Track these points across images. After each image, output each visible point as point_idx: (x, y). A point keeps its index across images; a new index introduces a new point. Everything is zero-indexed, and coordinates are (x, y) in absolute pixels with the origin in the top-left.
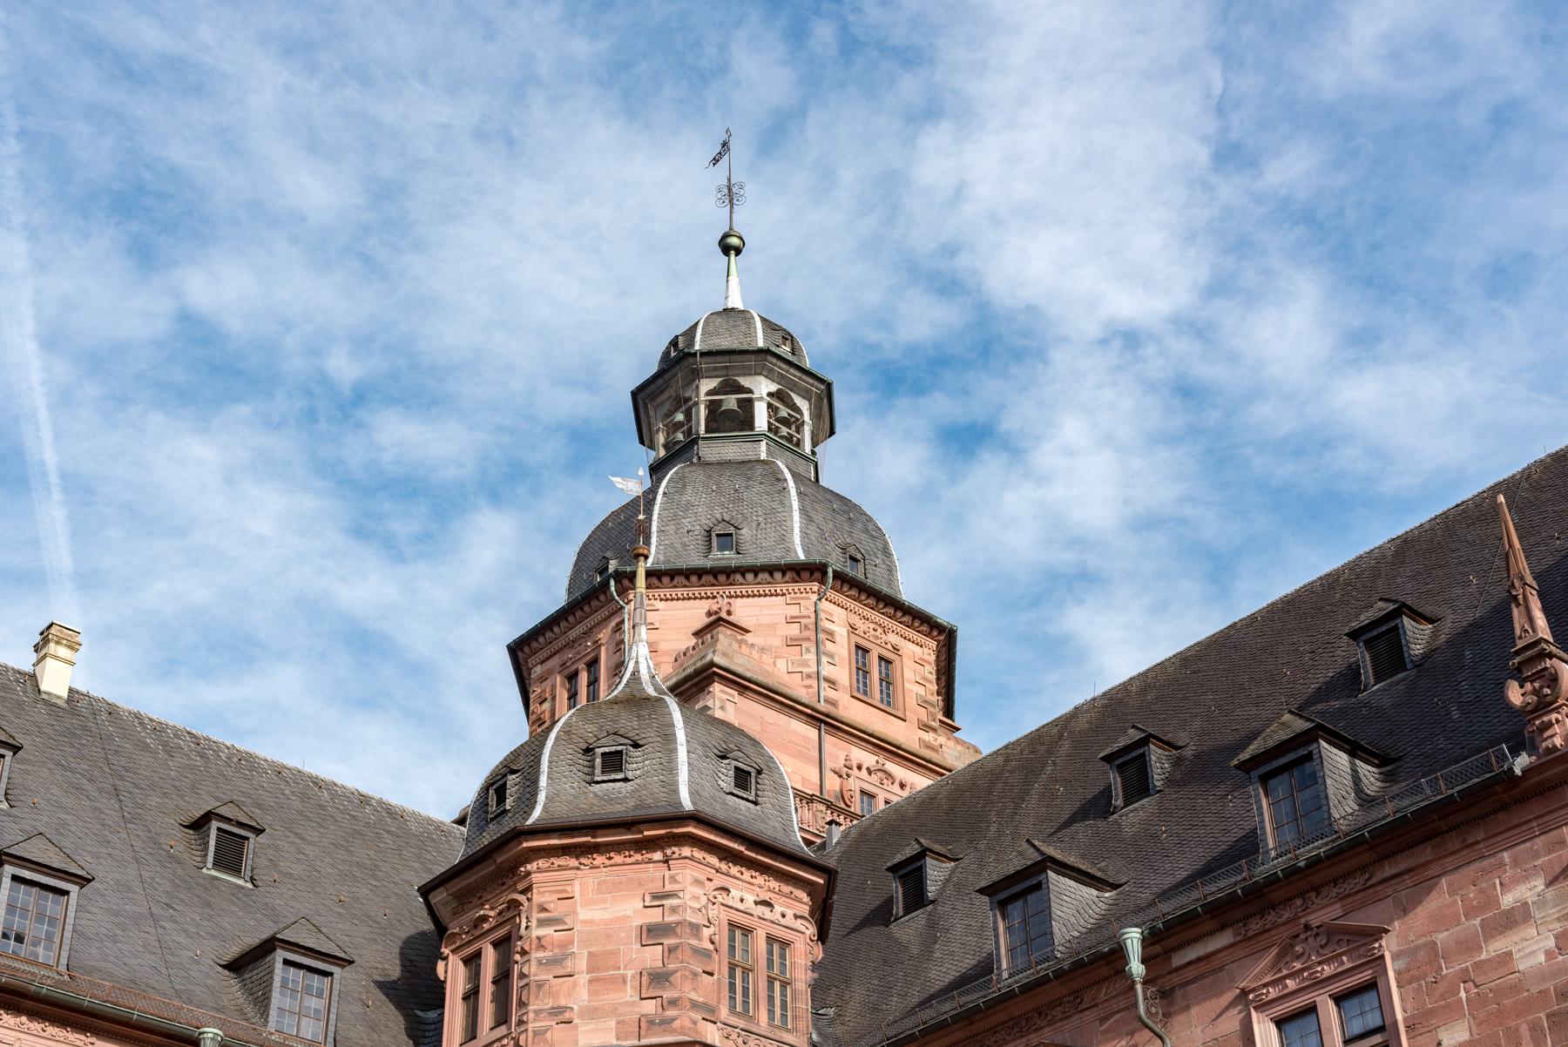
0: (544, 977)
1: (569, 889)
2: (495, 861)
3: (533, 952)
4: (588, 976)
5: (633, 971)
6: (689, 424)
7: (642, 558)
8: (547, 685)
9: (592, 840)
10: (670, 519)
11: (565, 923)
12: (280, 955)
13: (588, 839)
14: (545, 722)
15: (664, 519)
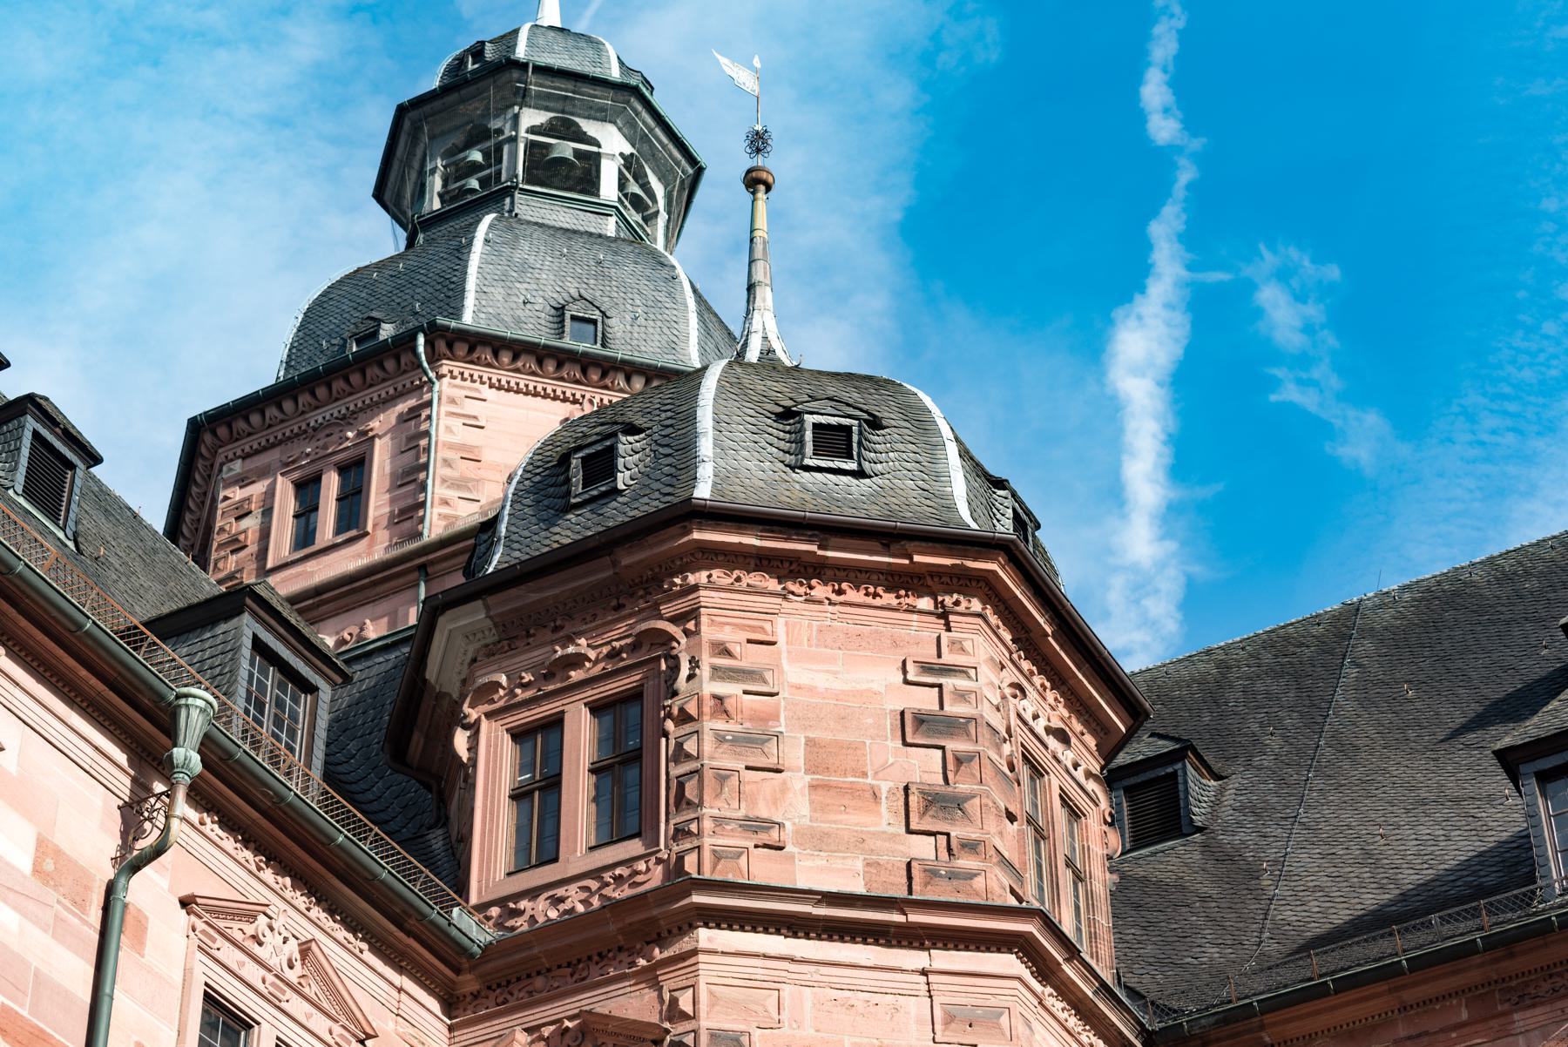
0: (729, 765)
1: (768, 626)
2: (615, 564)
3: (706, 718)
4: (808, 778)
5: (891, 784)
6: (498, 167)
7: (762, 188)
8: (258, 489)
9: (820, 553)
10: (496, 278)
11: (765, 682)
12: (247, 626)
13: (813, 548)
14: (246, 546)
15: (488, 277)
